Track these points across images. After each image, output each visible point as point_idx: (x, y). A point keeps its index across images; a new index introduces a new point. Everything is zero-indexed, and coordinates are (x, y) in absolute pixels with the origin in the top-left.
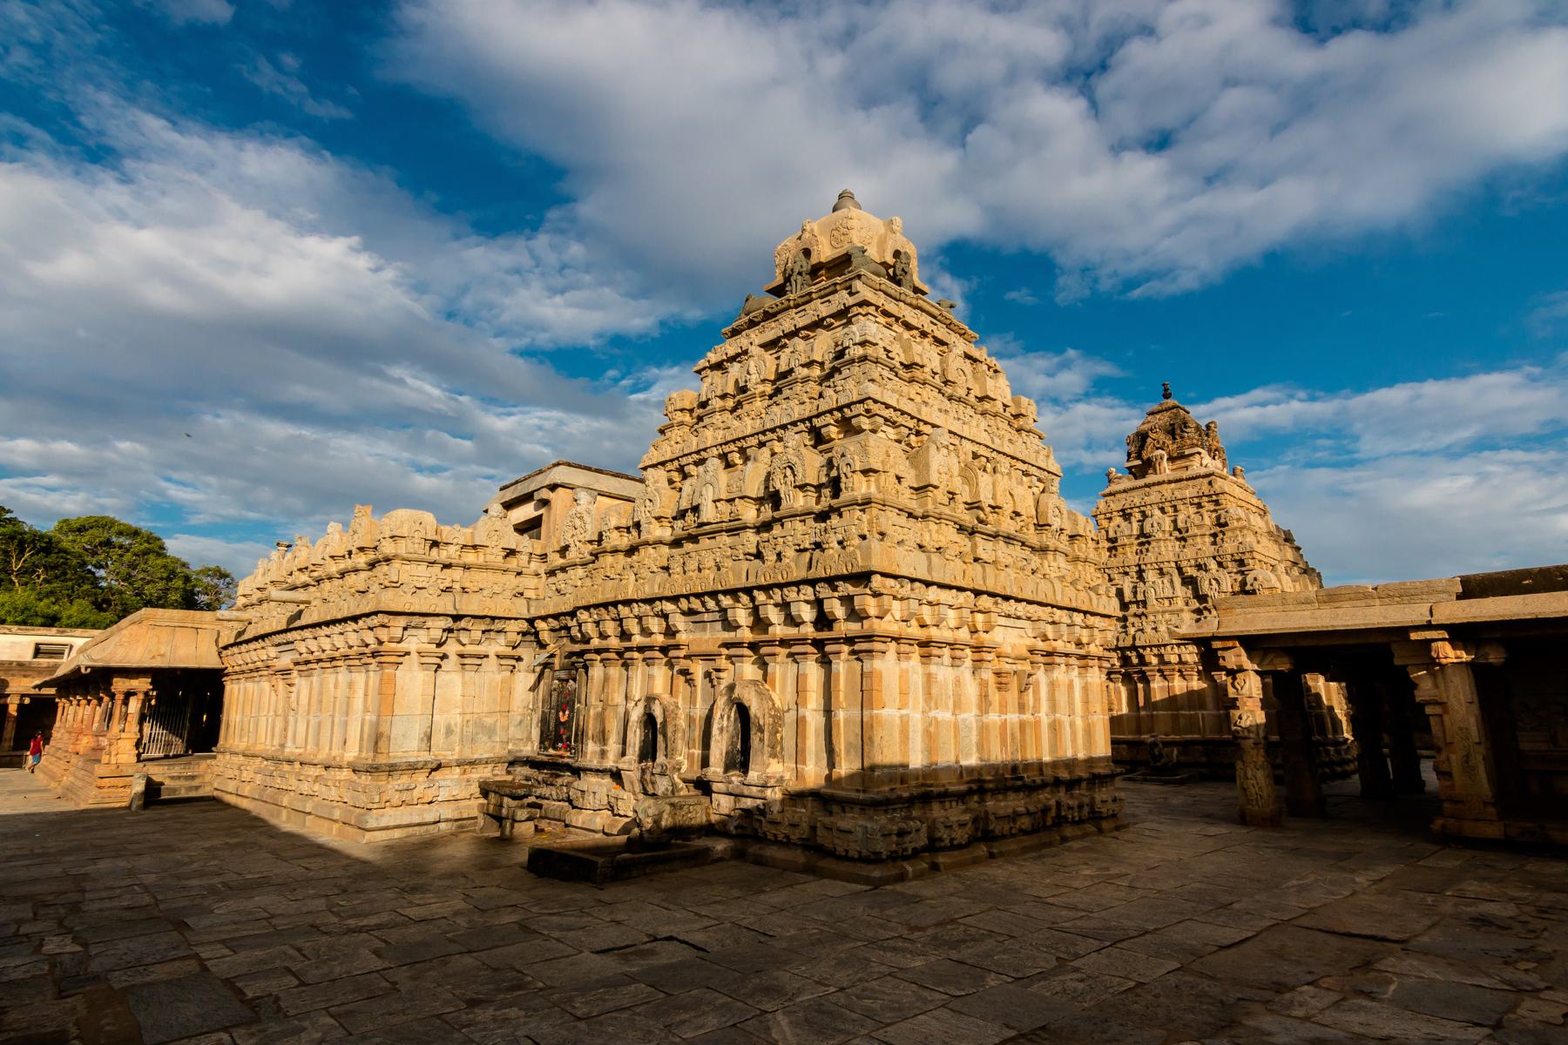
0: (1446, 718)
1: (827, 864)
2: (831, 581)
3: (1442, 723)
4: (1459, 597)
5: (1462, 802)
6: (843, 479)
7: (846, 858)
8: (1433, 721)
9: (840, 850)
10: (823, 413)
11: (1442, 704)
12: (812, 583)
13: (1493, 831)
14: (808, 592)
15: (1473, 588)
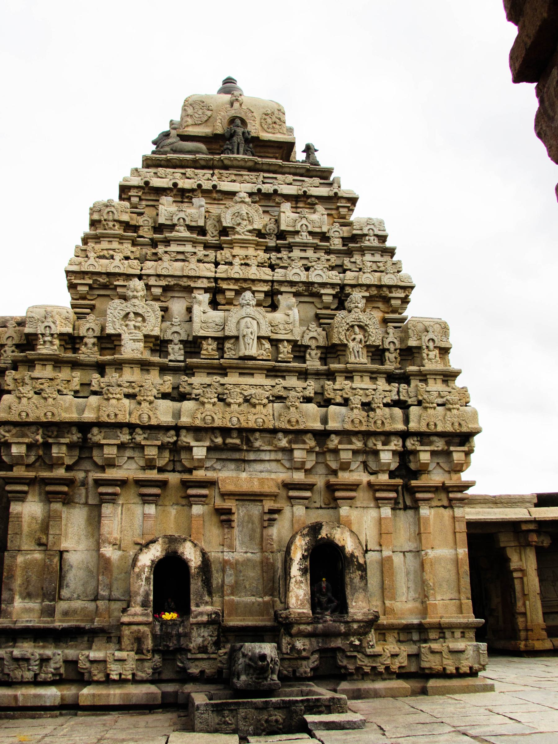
0: (525, 579)
1: (432, 683)
2: (424, 437)
3: (522, 583)
4: (536, 505)
5: (532, 630)
6: (426, 351)
7: (459, 675)
8: (517, 582)
9: (451, 669)
10: (361, 285)
11: (521, 570)
12: (404, 435)
13: (548, 645)
14: (396, 444)
15: (544, 500)
